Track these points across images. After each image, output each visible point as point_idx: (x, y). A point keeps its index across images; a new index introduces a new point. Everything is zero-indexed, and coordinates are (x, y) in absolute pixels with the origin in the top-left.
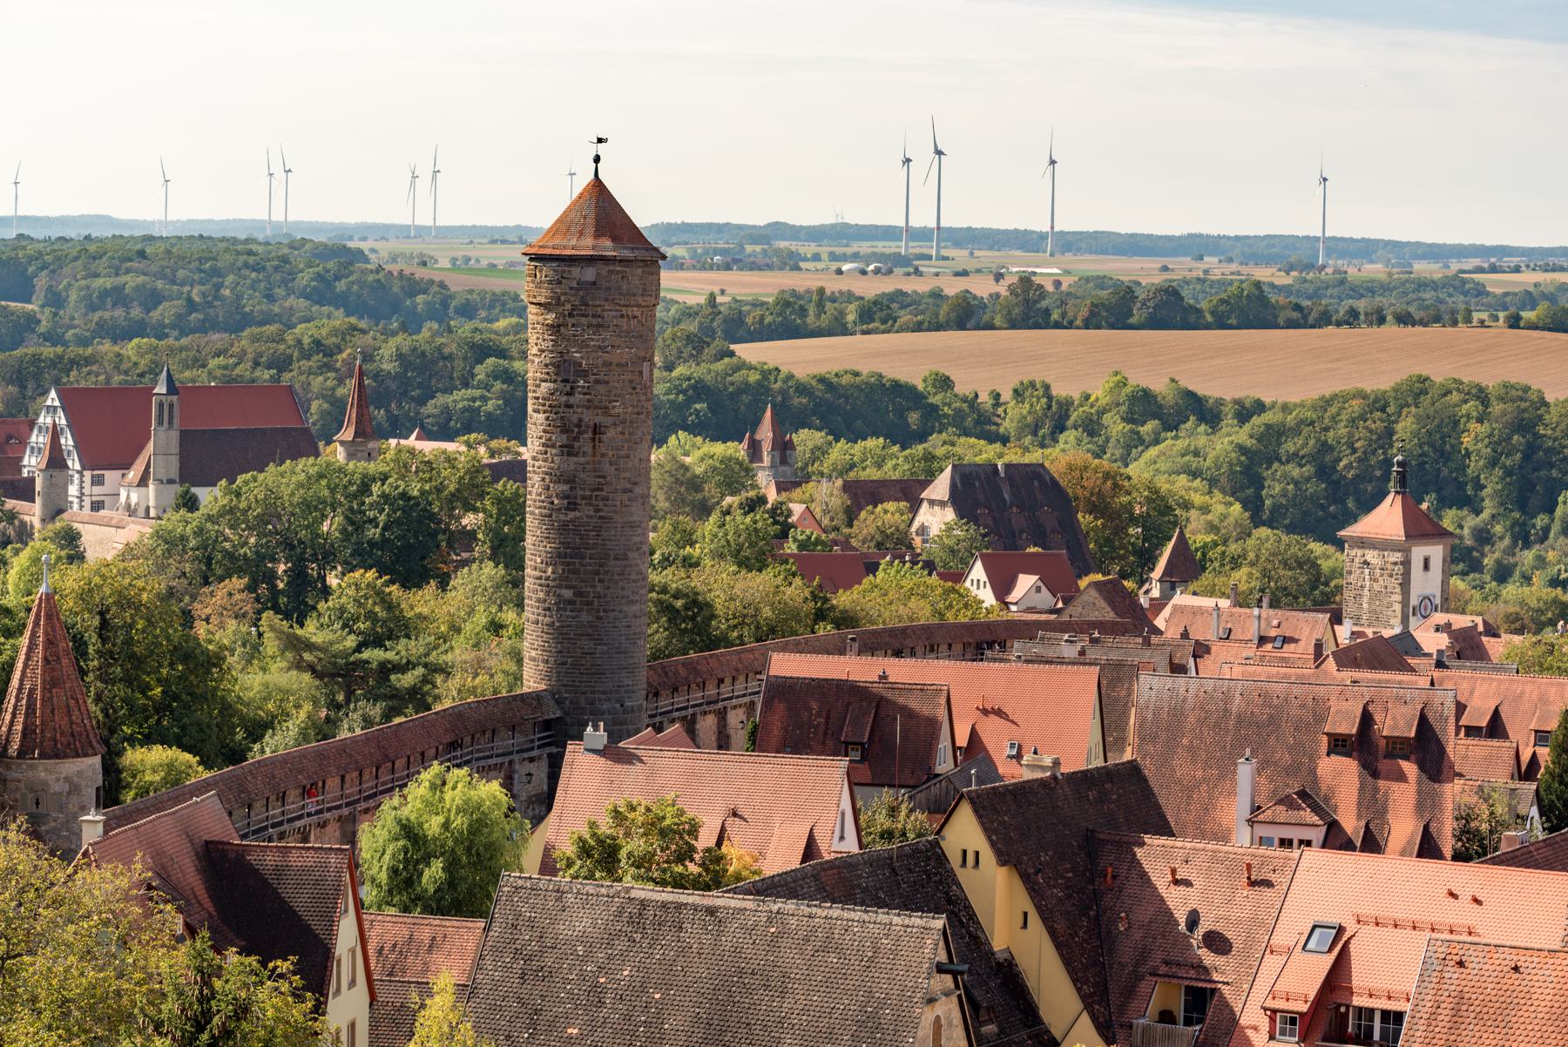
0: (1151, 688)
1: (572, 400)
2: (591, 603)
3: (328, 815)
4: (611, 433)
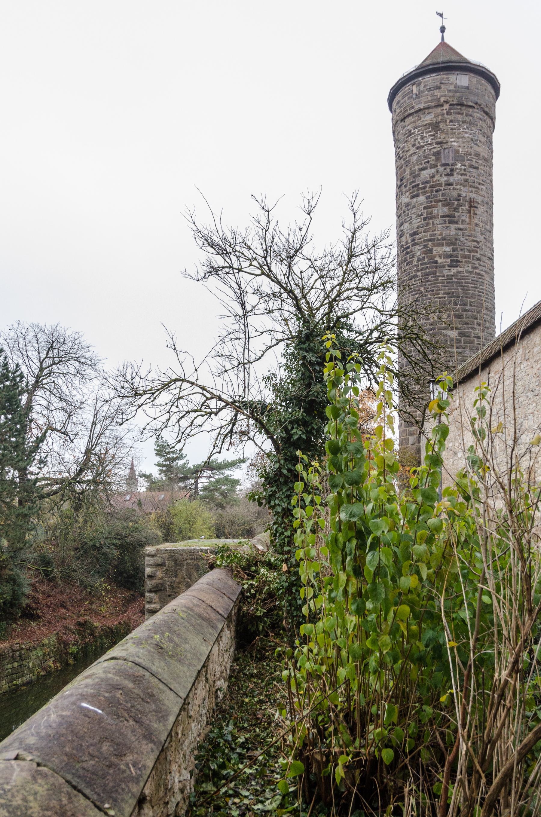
1: (451, 179)
2: (472, 343)
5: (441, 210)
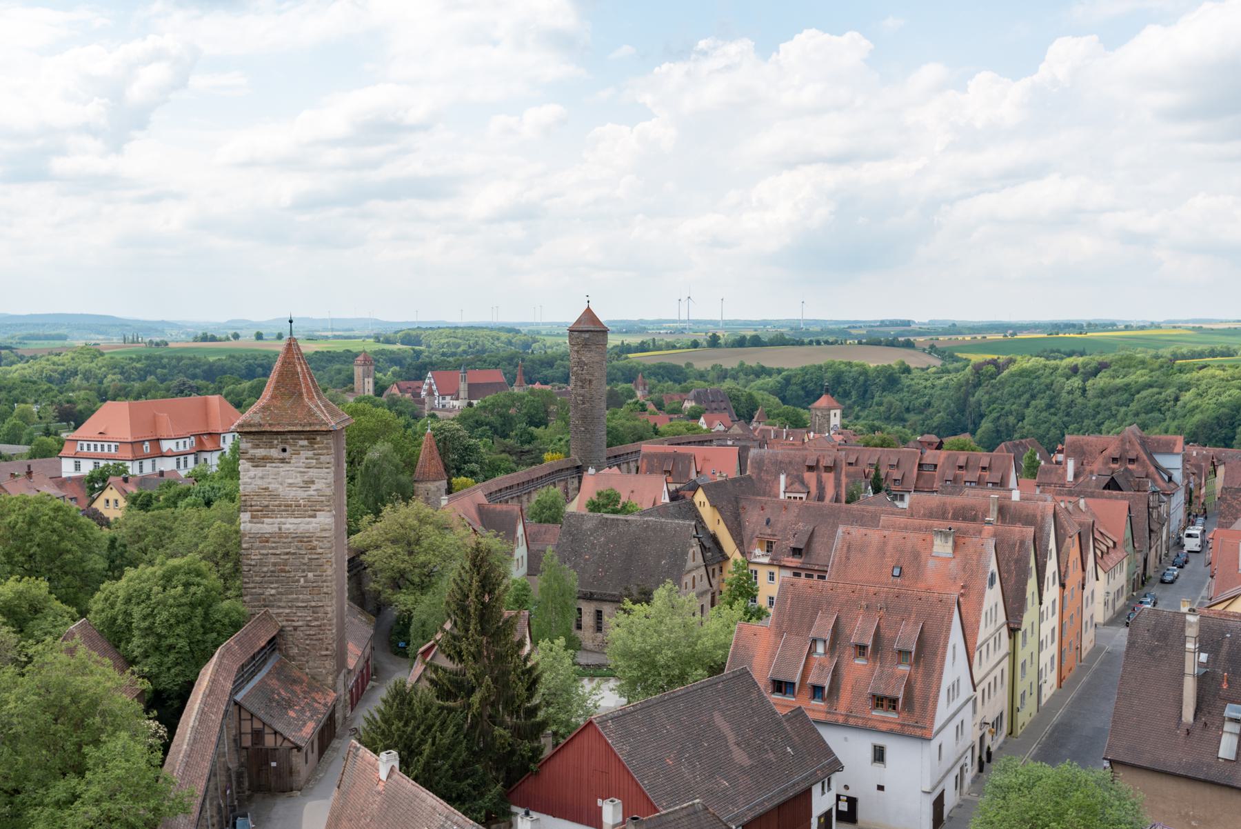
0: (753, 452)
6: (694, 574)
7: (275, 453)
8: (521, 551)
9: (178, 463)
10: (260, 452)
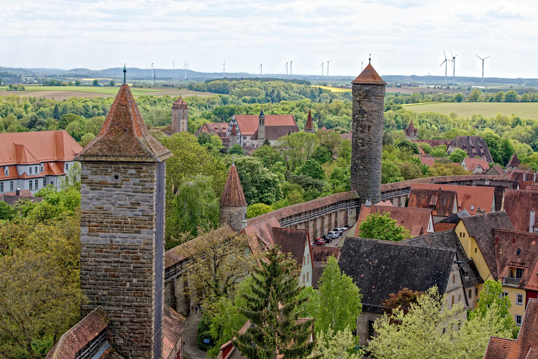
3: (302, 221)
4: (373, 128)
5: (360, 129)
6: (453, 293)
7: (109, 179)
8: (307, 268)
9: (31, 185)
10: (97, 178)
